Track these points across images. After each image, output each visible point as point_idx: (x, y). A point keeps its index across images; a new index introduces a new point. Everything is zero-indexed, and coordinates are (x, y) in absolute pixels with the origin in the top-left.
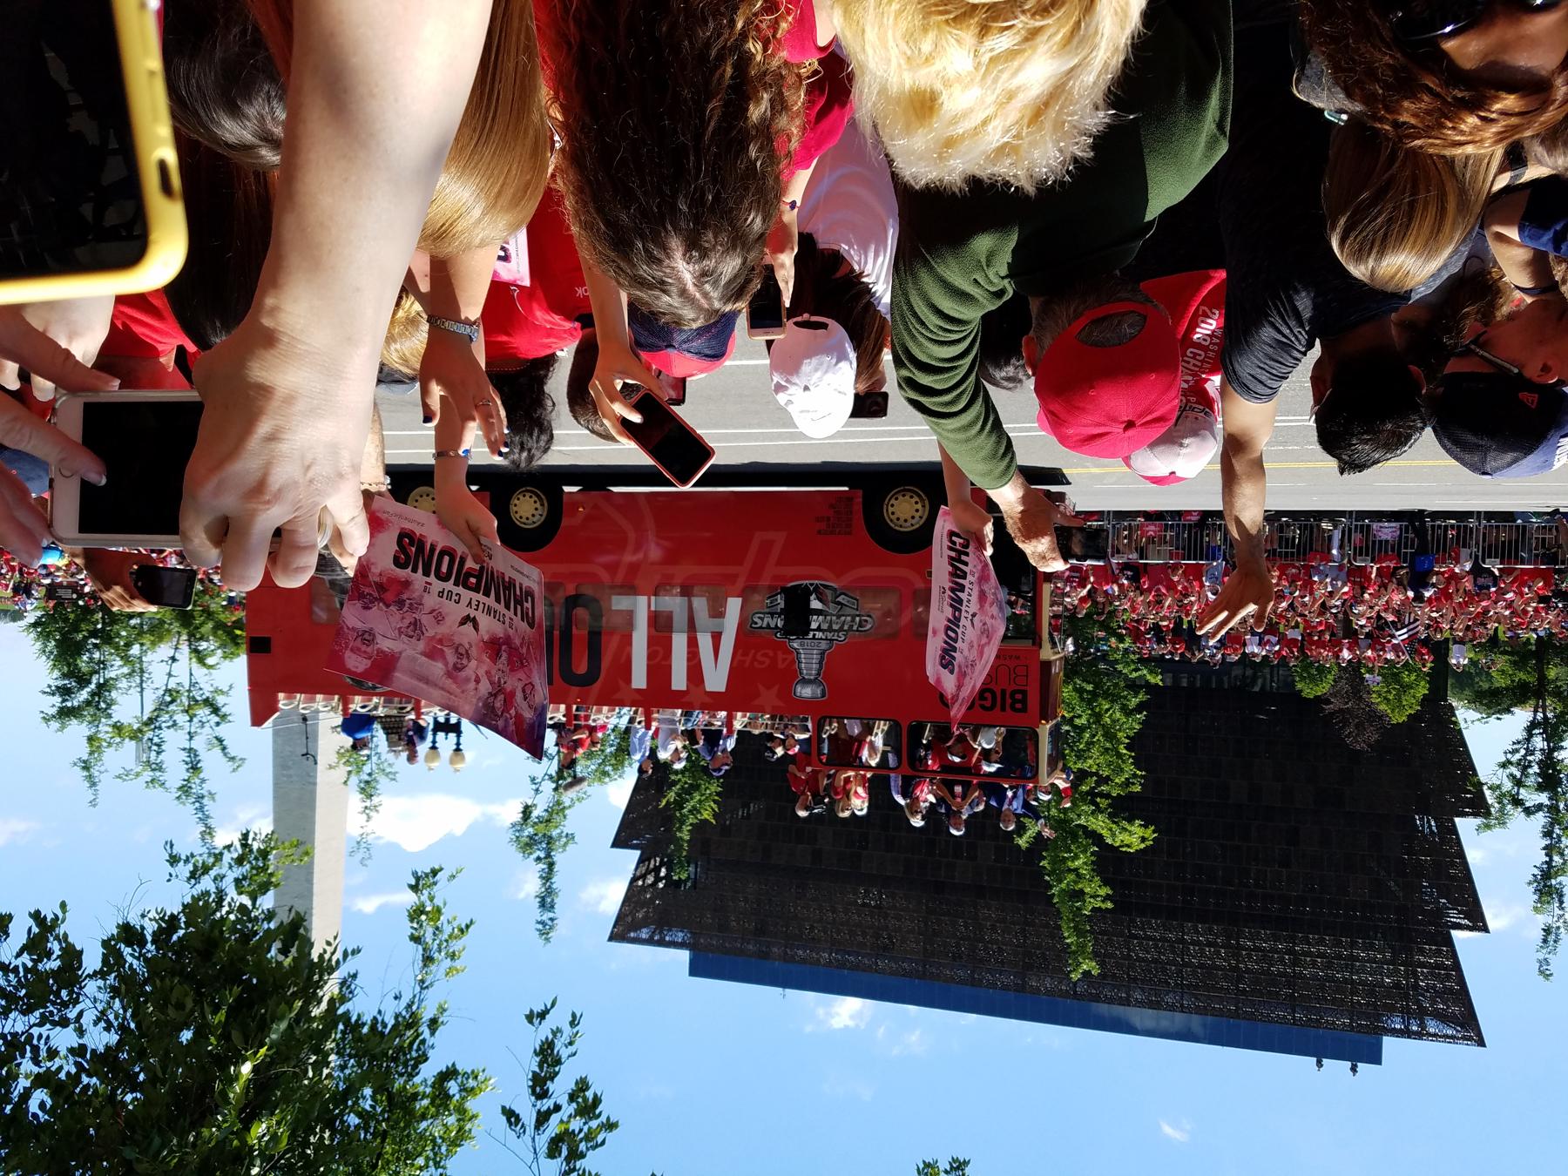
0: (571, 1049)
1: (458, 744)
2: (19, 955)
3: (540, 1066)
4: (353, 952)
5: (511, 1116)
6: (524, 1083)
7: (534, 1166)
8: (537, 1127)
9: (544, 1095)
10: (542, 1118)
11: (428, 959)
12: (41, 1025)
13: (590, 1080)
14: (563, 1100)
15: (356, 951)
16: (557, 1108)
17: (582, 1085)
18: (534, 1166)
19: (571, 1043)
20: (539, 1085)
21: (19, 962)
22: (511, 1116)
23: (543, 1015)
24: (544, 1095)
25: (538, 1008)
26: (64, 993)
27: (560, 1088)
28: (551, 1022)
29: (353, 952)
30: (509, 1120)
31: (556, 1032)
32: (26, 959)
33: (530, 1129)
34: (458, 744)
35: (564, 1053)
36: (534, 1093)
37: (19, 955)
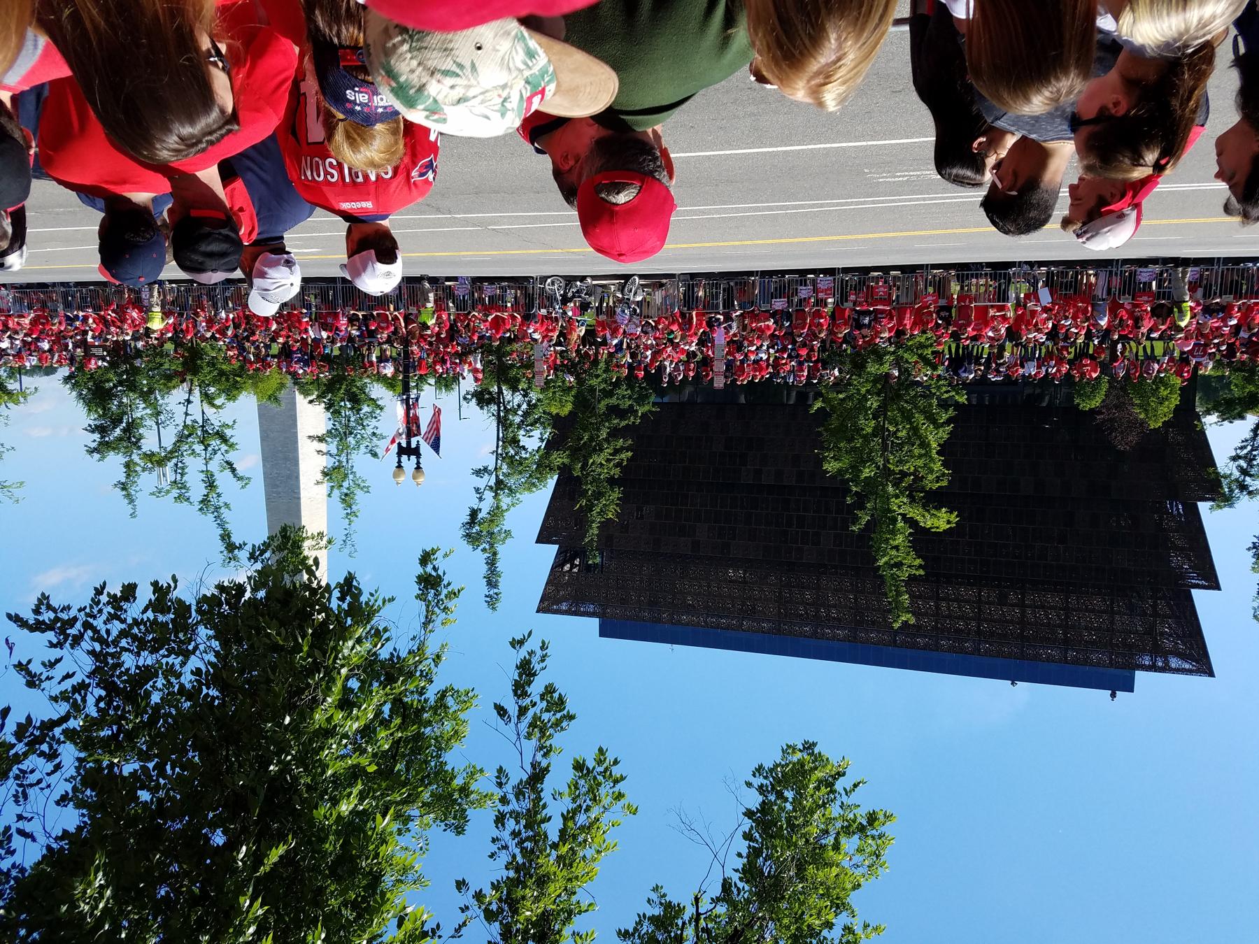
0: (543, 665)
3: (520, 675)
4: (389, 600)
5: (501, 711)
9: (525, 694)
10: (523, 711)
12: (168, 656)
13: (557, 686)
14: (537, 699)
15: (392, 599)
16: (534, 705)
17: (550, 690)
19: (543, 661)
20: (520, 689)
22: (501, 711)
23: (522, 642)
25: (519, 637)
26: (181, 635)
27: (536, 688)
28: (528, 646)
29: (389, 600)
30: (499, 713)
31: (531, 653)
32: (150, 614)
33: (514, 720)
35: (537, 667)
36: (515, 692)
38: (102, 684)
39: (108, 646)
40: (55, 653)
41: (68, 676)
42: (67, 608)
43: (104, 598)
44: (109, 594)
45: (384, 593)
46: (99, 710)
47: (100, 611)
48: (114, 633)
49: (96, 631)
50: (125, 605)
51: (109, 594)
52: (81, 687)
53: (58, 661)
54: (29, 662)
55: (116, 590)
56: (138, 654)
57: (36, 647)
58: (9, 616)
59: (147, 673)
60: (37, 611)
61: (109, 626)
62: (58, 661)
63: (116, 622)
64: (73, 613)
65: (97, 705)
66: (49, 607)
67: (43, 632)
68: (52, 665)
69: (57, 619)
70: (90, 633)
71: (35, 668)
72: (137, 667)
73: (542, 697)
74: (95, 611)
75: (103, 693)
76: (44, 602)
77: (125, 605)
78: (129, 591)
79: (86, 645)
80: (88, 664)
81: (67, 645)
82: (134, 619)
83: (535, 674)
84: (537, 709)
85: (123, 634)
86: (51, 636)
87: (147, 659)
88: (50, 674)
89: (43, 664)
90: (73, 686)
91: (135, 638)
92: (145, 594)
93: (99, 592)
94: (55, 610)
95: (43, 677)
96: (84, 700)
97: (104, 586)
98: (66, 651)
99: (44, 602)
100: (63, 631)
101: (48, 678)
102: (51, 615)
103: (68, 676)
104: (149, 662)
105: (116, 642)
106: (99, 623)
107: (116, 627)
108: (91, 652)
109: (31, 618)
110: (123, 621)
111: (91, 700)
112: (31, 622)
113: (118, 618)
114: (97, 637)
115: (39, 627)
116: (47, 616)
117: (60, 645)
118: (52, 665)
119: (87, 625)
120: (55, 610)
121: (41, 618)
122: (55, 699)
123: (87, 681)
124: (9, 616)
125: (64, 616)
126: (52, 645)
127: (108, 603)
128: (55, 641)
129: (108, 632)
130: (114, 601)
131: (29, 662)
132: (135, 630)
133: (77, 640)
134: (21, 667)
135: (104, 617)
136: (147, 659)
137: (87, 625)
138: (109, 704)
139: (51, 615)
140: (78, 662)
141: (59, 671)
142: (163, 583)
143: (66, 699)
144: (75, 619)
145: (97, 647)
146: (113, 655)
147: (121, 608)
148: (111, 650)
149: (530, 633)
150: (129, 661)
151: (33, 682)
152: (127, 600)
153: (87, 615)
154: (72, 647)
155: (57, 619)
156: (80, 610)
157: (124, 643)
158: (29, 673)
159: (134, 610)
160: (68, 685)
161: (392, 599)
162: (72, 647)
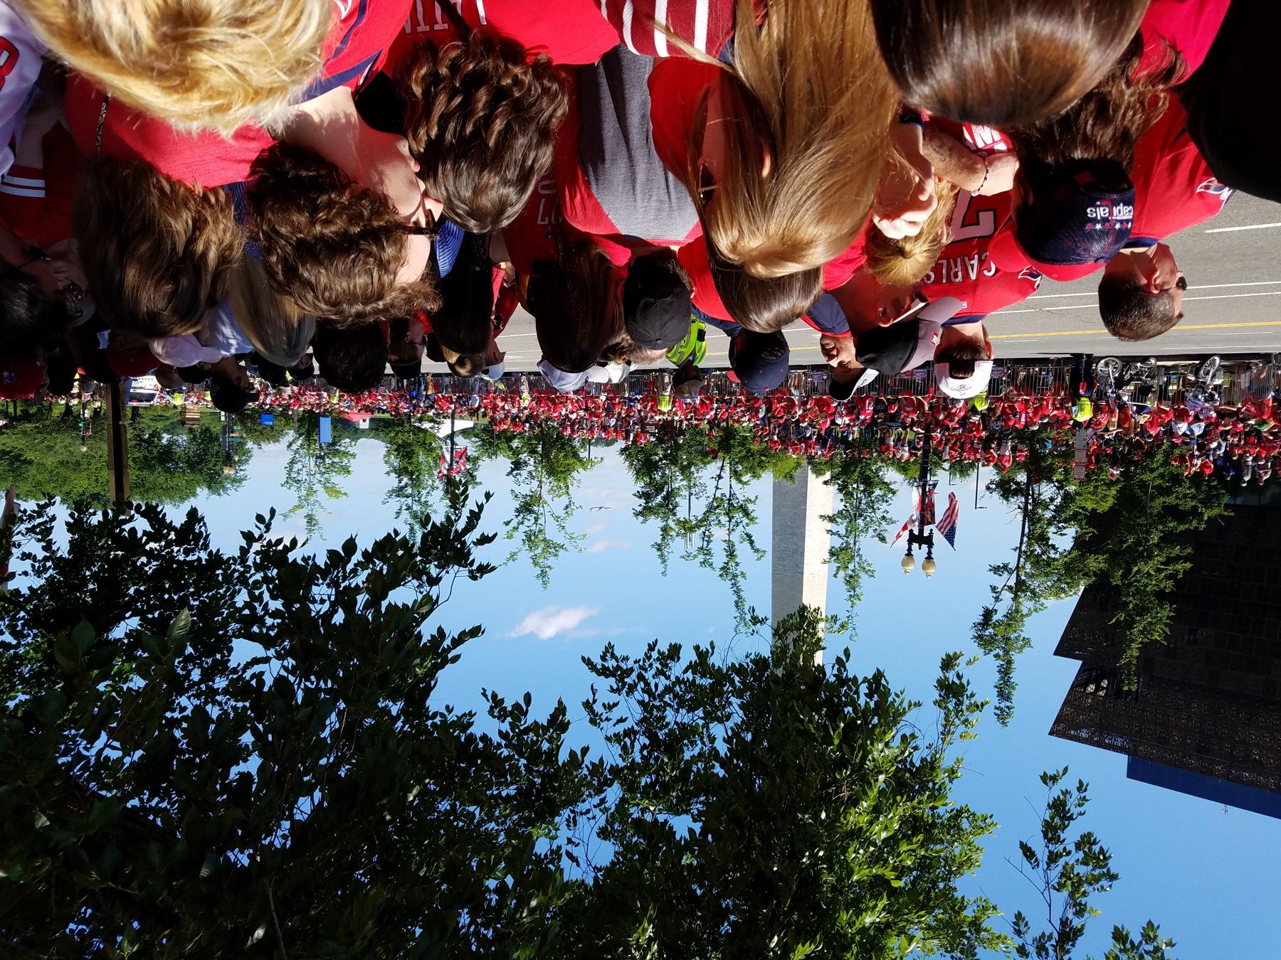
0: (1082, 809)
1: (930, 553)
2: (685, 672)
3: (1052, 818)
5: (1028, 852)
6: (1038, 829)
7: (1046, 893)
8: (1049, 865)
9: (1058, 840)
10: (1053, 858)
11: (948, 723)
13: (1097, 835)
14: (1071, 847)
16: (1069, 853)
17: (1086, 841)
18: (1046, 893)
20: (1051, 832)
21: (685, 676)
22: (1028, 852)
23: (1054, 779)
24: (1058, 840)
25: (1051, 772)
27: (1071, 835)
28: (1062, 784)
30: (1025, 854)
31: (1065, 793)
32: (689, 675)
33: (1043, 865)
34: (930, 553)
36: (1045, 836)
37: (685, 672)
40: (614, 698)
41: (621, 720)
42: (626, 659)
43: (655, 655)
45: (909, 697)
46: (643, 757)
47: (651, 665)
48: (661, 688)
49: (647, 684)
52: (629, 733)
53: (615, 705)
55: (663, 647)
56: (677, 711)
58: (583, 658)
60: (603, 658)
62: (615, 705)
63: (662, 678)
64: (630, 664)
66: (613, 656)
68: (610, 707)
69: (618, 667)
70: (642, 684)
71: (598, 708)
72: (676, 723)
73: (1078, 846)
75: (647, 742)
78: (675, 651)
79: (638, 694)
80: (638, 712)
82: (677, 678)
83: (1071, 818)
84: (1071, 860)
85: (668, 690)
86: (612, 681)
87: (684, 717)
88: (610, 715)
91: (676, 695)
92: (688, 656)
93: (652, 647)
95: (603, 717)
96: (633, 747)
97: (655, 643)
100: (621, 679)
101: (608, 719)
103: (621, 720)
105: (661, 697)
106: (648, 675)
107: (663, 682)
108: (641, 703)
110: (668, 678)
111: (637, 747)
112: (599, 667)
113: (664, 674)
114: (647, 690)
115: (604, 672)
116: (611, 663)
117: (618, 691)
118: (610, 707)
119: (641, 677)
122: (608, 739)
123: (636, 728)
124: (583, 658)
126: (612, 690)
127: (658, 659)
128: (615, 687)
129: (656, 685)
132: (677, 688)
133: (632, 688)
135: (653, 671)
136: (684, 717)
137: (641, 677)
140: (630, 709)
141: (615, 714)
142: (702, 648)
143: (619, 741)
144: (632, 670)
145: (646, 696)
146: (658, 708)
147: (666, 665)
148: (657, 703)
149: (1066, 769)
150: (670, 715)
151: (595, 720)
153: (641, 667)
155: (618, 667)
157: (667, 699)
159: (677, 669)
160: (620, 728)
161: (918, 704)
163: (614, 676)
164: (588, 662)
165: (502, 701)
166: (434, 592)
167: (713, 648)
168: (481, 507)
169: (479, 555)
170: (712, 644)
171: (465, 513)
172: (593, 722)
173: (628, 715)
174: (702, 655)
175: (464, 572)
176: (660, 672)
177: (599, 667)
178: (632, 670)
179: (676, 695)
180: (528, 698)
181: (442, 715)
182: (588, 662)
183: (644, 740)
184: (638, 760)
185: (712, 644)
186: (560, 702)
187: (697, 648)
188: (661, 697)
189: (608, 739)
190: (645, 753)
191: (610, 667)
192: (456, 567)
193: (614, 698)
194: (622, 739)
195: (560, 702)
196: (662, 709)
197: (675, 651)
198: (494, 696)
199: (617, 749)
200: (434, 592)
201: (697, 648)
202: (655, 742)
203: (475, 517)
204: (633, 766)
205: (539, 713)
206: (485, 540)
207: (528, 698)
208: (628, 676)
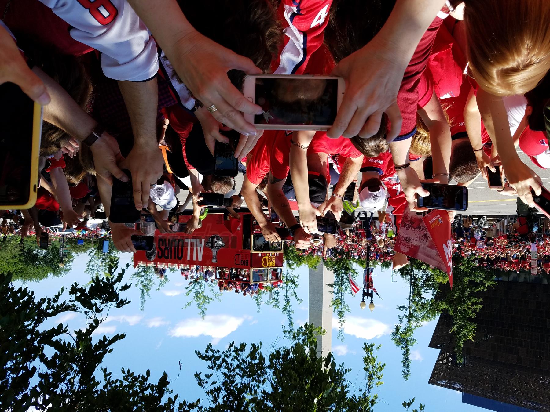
1: (372, 301)
2: (247, 357)
12: (253, 381)
21: (247, 360)
26: (259, 372)
32: (249, 359)
34: (372, 301)
37: (247, 357)
38: (227, 389)
39: (231, 371)
40: (210, 372)
41: (214, 383)
42: (219, 351)
43: (233, 349)
44: (235, 347)
46: (224, 401)
47: (230, 354)
49: (227, 364)
50: (241, 353)
51: (235, 347)
52: (218, 390)
53: (211, 375)
54: (200, 373)
57: (203, 367)
58: (196, 352)
59: (246, 387)
60: (207, 351)
61: (233, 362)
62: (211, 375)
63: (236, 360)
64: (220, 353)
65: (223, 399)
66: (212, 350)
67: (207, 360)
68: (208, 376)
69: (213, 356)
70: (224, 364)
71: (202, 377)
72: (242, 384)
74: (228, 354)
76: (209, 348)
77: (241, 353)
78: (243, 346)
79: (222, 369)
81: (215, 368)
82: (242, 360)
85: (237, 367)
87: (246, 380)
88: (207, 381)
89: (206, 375)
90: (215, 388)
91: (242, 369)
92: (248, 350)
93: (231, 345)
94: (213, 351)
95: (205, 382)
97: (233, 344)
98: (214, 371)
99: (209, 348)
100: (214, 362)
101: (206, 382)
102: (211, 354)
103: (214, 383)
104: (247, 382)
105: (234, 370)
106: (229, 360)
107: (235, 363)
108: (224, 374)
109: (203, 353)
110: (239, 361)
111: (221, 396)
112: (204, 355)
113: (237, 359)
114: (227, 367)
116: (210, 354)
117: (212, 368)
118: (208, 376)
119: (224, 360)
120: (213, 351)
121: (207, 354)
122: (208, 393)
123: (221, 386)
124: (196, 352)
125: (216, 355)
126: (210, 368)
127: (234, 351)
128: (211, 366)
129: (231, 365)
130: (236, 350)
131: (200, 373)
132: (242, 366)
133: (220, 366)
134: (197, 375)
136: (246, 380)
137: (224, 360)
138: (228, 399)
139: (211, 354)
140: (218, 377)
141: (211, 380)
143: (212, 394)
144: (220, 357)
145: (227, 371)
146: (232, 376)
147: (238, 354)
148: (232, 374)
150: (238, 380)
152: (241, 351)
153: (225, 356)
154: (217, 369)
155: (213, 356)
156: (223, 353)
157: (237, 371)
158: (200, 378)
159: (244, 355)
160: (213, 387)
162: (217, 369)
163: (210, 360)
164: (198, 353)
165: (133, 373)
166: (99, 316)
167: (261, 345)
168: (123, 271)
169: (122, 295)
170: (261, 343)
171: (116, 274)
172: (200, 384)
173: (217, 380)
174: (255, 349)
175: (114, 304)
176: (235, 358)
177: (204, 355)
178: (220, 357)
179: (242, 369)
180: (148, 373)
181: (121, 382)
182: (198, 353)
183: (225, 393)
184: (221, 403)
185: (261, 343)
186: (165, 373)
187: (253, 345)
188: (234, 370)
189: (208, 393)
190: (225, 399)
191: (210, 356)
192: (111, 303)
193: (210, 372)
194: (214, 393)
195: (165, 373)
196: (234, 376)
197: (243, 346)
198: (129, 371)
199: (211, 398)
200: (99, 316)
201: (253, 345)
202: (230, 393)
203: (120, 276)
204: (218, 406)
205: (154, 380)
206: (125, 288)
207: (148, 373)
208: (219, 360)
